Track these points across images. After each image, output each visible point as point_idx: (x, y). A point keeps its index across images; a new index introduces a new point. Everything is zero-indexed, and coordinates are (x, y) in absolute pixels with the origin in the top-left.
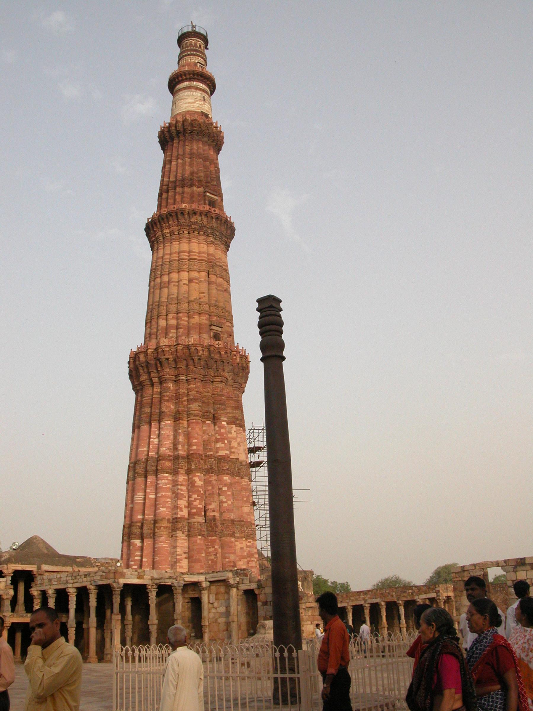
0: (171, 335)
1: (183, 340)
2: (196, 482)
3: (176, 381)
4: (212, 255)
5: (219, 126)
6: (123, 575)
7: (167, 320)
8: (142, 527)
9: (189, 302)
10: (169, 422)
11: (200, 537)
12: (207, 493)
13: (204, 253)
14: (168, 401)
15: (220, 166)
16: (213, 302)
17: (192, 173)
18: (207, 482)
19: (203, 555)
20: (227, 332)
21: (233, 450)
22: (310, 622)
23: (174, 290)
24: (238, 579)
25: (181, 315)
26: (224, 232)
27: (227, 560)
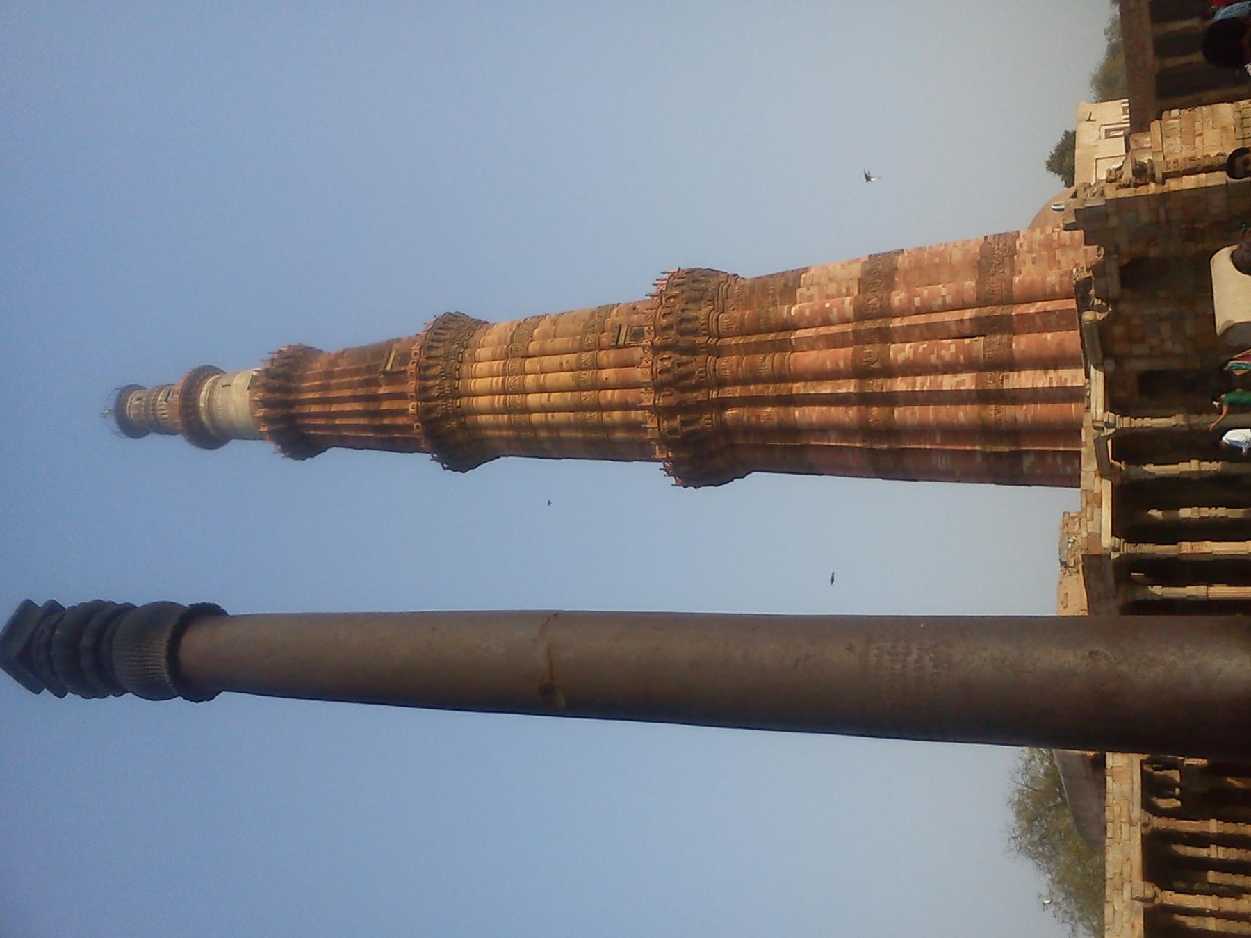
0: (640, 418)
1: (648, 398)
2: (907, 359)
3: (724, 404)
4: (494, 353)
5: (270, 356)
6: (1095, 538)
7: (614, 427)
8: (999, 455)
9: (579, 388)
10: (797, 414)
11: (1014, 345)
12: (927, 335)
13: (491, 367)
14: (758, 417)
15: (341, 350)
16: (576, 345)
17: (355, 399)
18: (907, 335)
19: (1049, 336)
20: (628, 314)
21: (844, 291)
22: (1198, 139)
23: (560, 417)
24: (1097, 302)
25: (602, 401)
26: (452, 334)
27: (1057, 288)
